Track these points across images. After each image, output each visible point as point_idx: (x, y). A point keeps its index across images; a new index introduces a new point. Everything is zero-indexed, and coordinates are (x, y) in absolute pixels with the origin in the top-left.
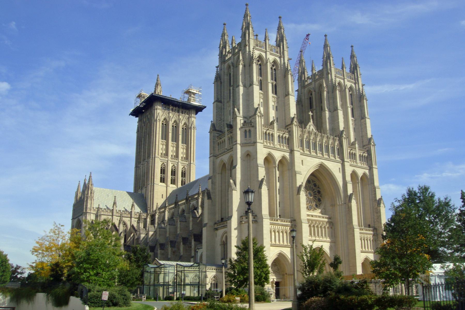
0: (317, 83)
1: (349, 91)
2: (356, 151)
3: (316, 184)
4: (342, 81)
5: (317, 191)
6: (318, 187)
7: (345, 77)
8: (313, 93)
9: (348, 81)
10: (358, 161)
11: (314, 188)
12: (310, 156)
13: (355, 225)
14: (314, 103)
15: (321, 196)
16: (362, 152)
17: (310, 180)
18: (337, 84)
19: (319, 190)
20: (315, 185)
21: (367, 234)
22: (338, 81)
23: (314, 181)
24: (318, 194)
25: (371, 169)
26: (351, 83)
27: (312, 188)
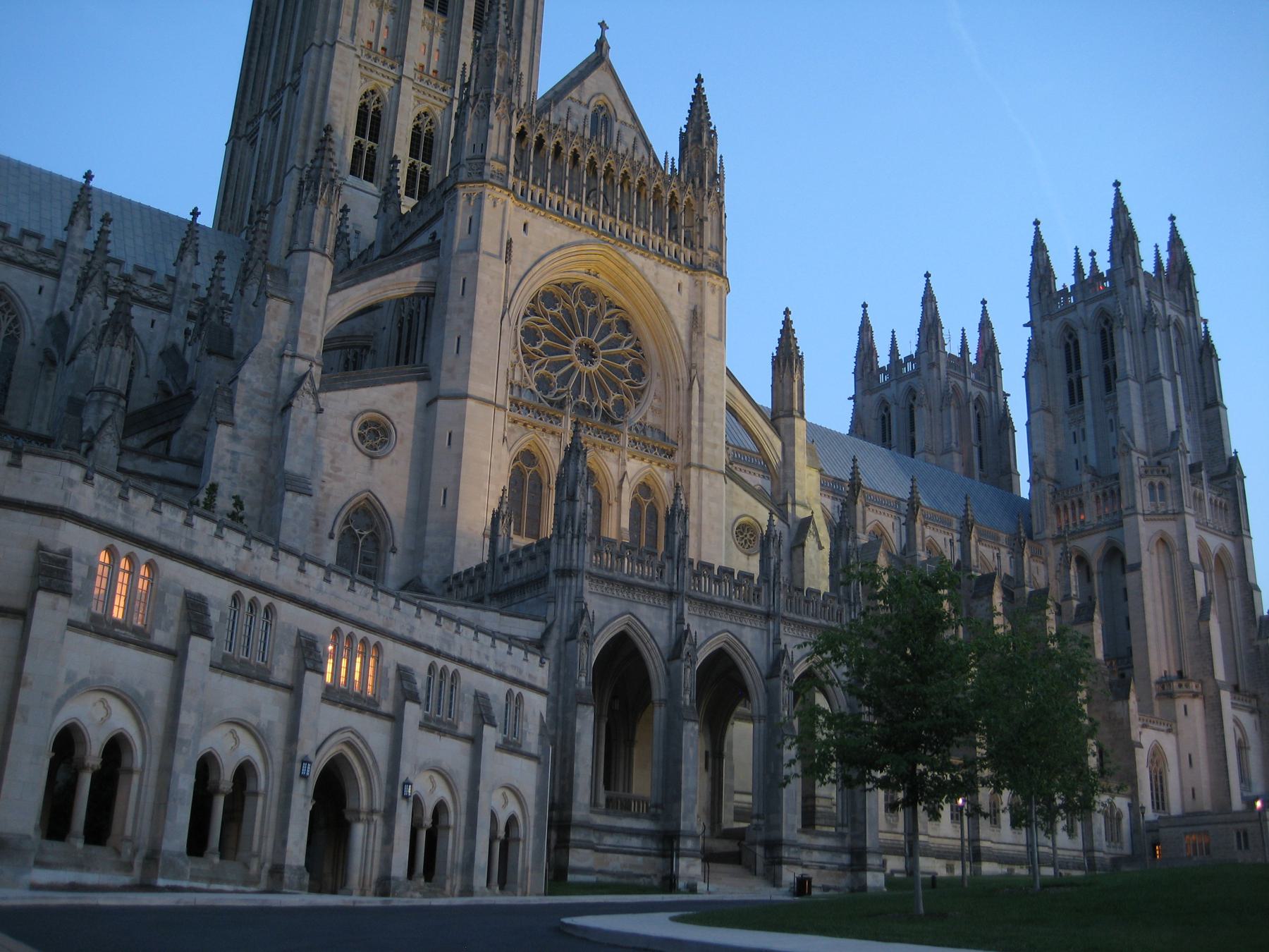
0: (903, 385)
1: (976, 408)
4: (961, 383)
7: (968, 376)
8: (893, 409)
9: (973, 383)
14: (894, 433)
18: (951, 391)
22: (953, 384)
26: (978, 390)
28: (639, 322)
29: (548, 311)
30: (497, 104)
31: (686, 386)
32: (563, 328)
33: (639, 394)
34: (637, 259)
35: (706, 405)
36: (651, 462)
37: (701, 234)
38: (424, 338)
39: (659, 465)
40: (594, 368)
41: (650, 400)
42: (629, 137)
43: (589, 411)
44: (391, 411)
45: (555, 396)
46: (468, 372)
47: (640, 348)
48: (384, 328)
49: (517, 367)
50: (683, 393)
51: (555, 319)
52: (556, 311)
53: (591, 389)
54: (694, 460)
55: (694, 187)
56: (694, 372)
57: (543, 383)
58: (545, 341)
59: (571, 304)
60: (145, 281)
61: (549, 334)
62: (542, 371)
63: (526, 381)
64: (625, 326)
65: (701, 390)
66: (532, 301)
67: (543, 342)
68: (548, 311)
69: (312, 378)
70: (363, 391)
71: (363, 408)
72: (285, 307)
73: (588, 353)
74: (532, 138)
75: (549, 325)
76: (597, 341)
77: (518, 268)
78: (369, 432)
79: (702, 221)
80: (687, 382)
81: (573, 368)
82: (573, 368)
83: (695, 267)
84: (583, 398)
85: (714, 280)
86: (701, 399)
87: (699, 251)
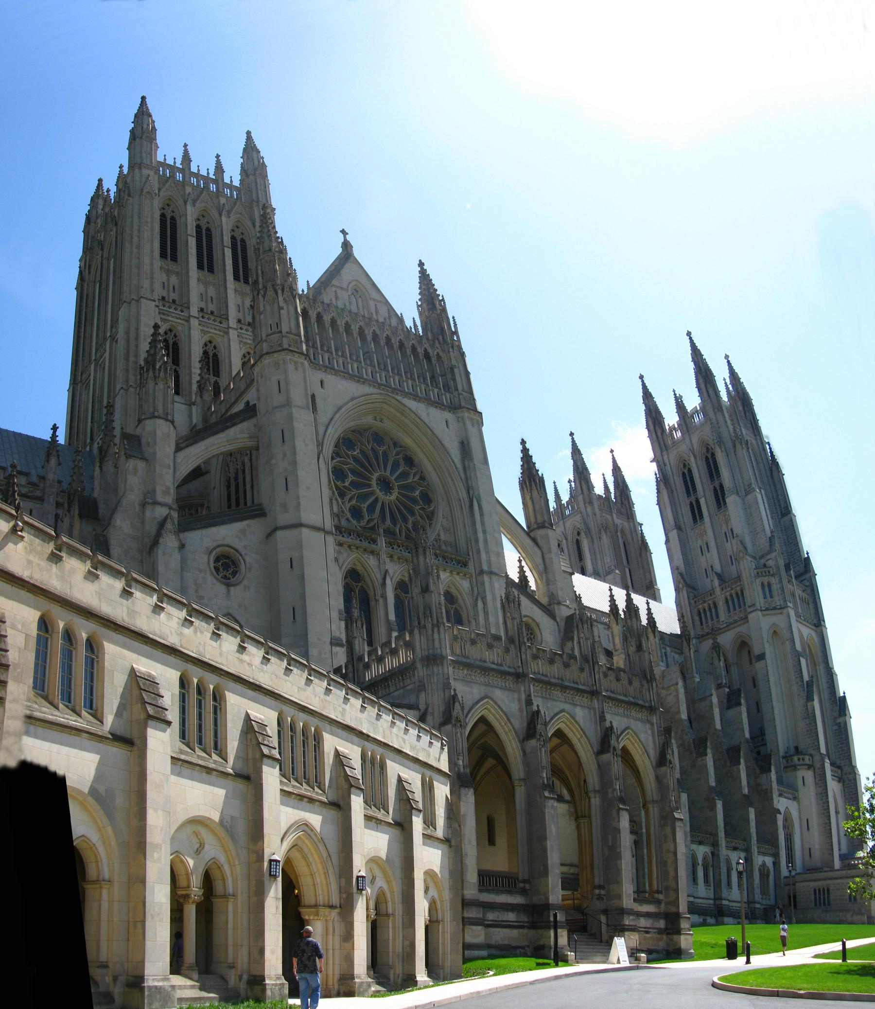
28: (421, 457)
29: (350, 453)
30: (283, 290)
31: (467, 504)
32: (363, 466)
33: (431, 516)
34: (411, 404)
35: (486, 519)
36: (451, 572)
37: (454, 380)
38: (252, 487)
39: (458, 574)
40: (393, 497)
41: (440, 521)
42: (383, 311)
43: (394, 534)
44: (239, 544)
45: (367, 524)
46: (299, 504)
47: (425, 479)
48: (214, 488)
49: (334, 501)
50: (466, 511)
51: (355, 459)
52: (355, 453)
53: (393, 517)
54: (485, 567)
55: (440, 343)
56: (471, 493)
57: (356, 513)
58: (351, 478)
59: (366, 447)
60: (23, 480)
61: (354, 472)
62: (354, 502)
63: (343, 512)
64: (410, 461)
65: (480, 507)
66: (336, 446)
67: (350, 479)
68: (350, 453)
69: (172, 519)
70: (213, 530)
71: (215, 544)
72: (141, 464)
73: (386, 485)
74: (313, 314)
75: (352, 464)
76: (392, 473)
77: (323, 419)
78: (222, 565)
79: (452, 369)
80: (467, 500)
81: (376, 500)
82: (376, 500)
83: (454, 408)
84: (388, 522)
85: (472, 415)
86: (482, 514)
87: (456, 393)
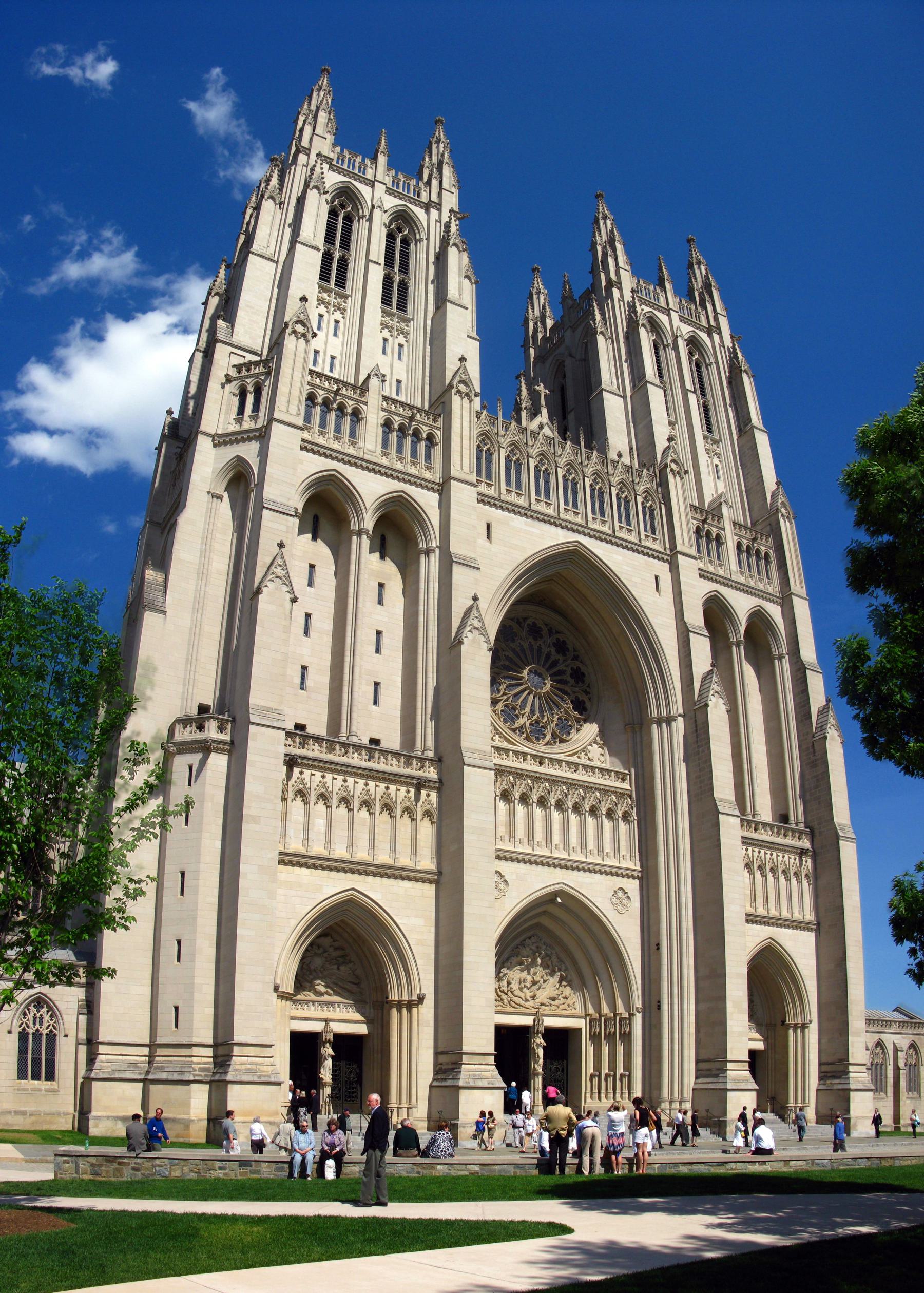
2: (724, 529)
3: (564, 641)
5: (569, 671)
6: (576, 658)
10: (734, 566)
11: (555, 656)
12: (526, 512)
13: (721, 800)
15: (587, 693)
16: (746, 538)
17: (540, 624)
19: (578, 668)
20: (561, 647)
21: (772, 846)
23: (557, 632)
24: (572, 681)
25: (786, 601)
27: (548, 656)
